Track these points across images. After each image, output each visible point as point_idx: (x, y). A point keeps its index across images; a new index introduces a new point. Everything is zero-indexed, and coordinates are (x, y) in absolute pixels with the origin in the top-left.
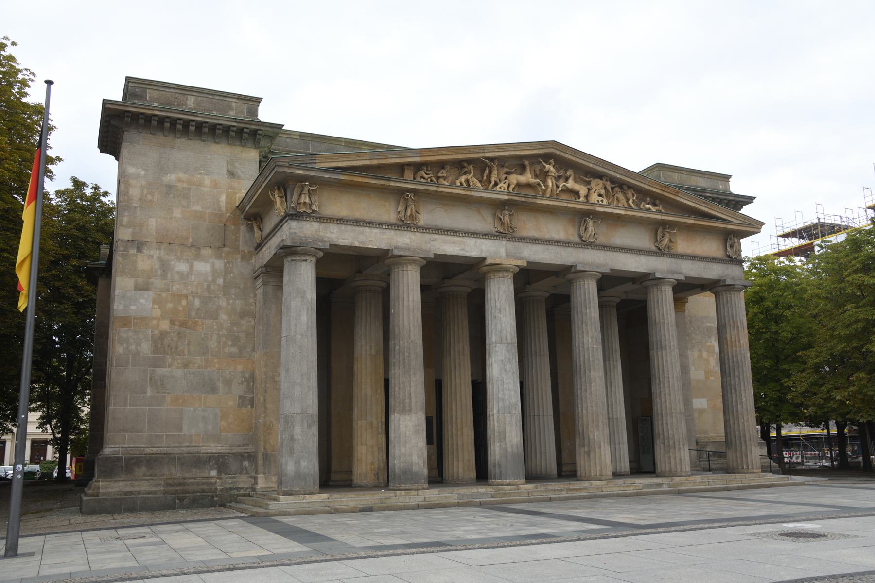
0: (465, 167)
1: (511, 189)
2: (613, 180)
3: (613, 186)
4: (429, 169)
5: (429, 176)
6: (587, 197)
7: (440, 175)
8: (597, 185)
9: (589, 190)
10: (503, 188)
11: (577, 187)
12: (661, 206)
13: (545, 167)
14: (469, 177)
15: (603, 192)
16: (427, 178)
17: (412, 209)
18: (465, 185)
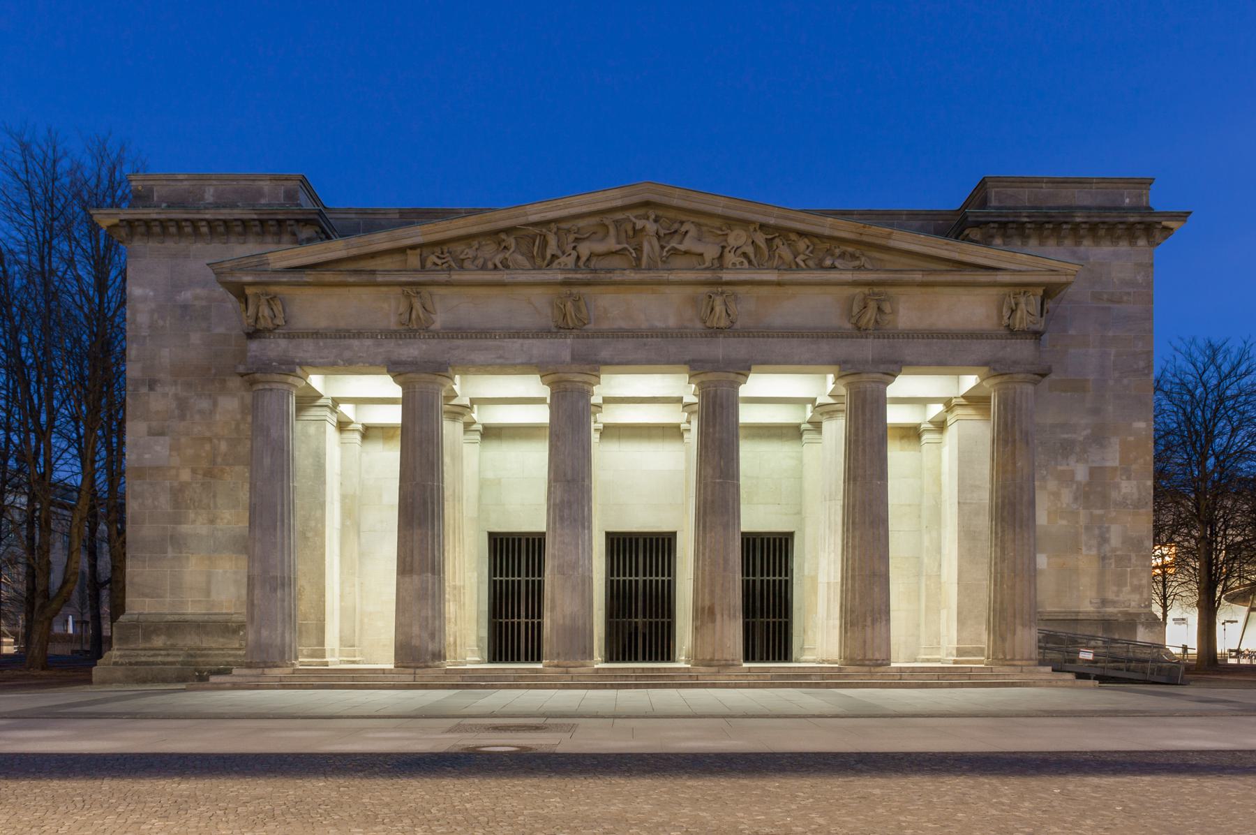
0: (504, 240)
1: (581, 263)
2: (763, 227)
3: (770, 237)
4: (446, 250)
5: (444, 261)
6: (721, 256)
7: (462, 257)
8: (737, 238)
9: (723, 247)
10: (563, 265)
11: (698, 248)
12: (863, 259)
13: (634, 224)
14: (507, 256)
15: (750, 250)
16: (440, 263)
17: (417, 311)
18: (499, 265)
